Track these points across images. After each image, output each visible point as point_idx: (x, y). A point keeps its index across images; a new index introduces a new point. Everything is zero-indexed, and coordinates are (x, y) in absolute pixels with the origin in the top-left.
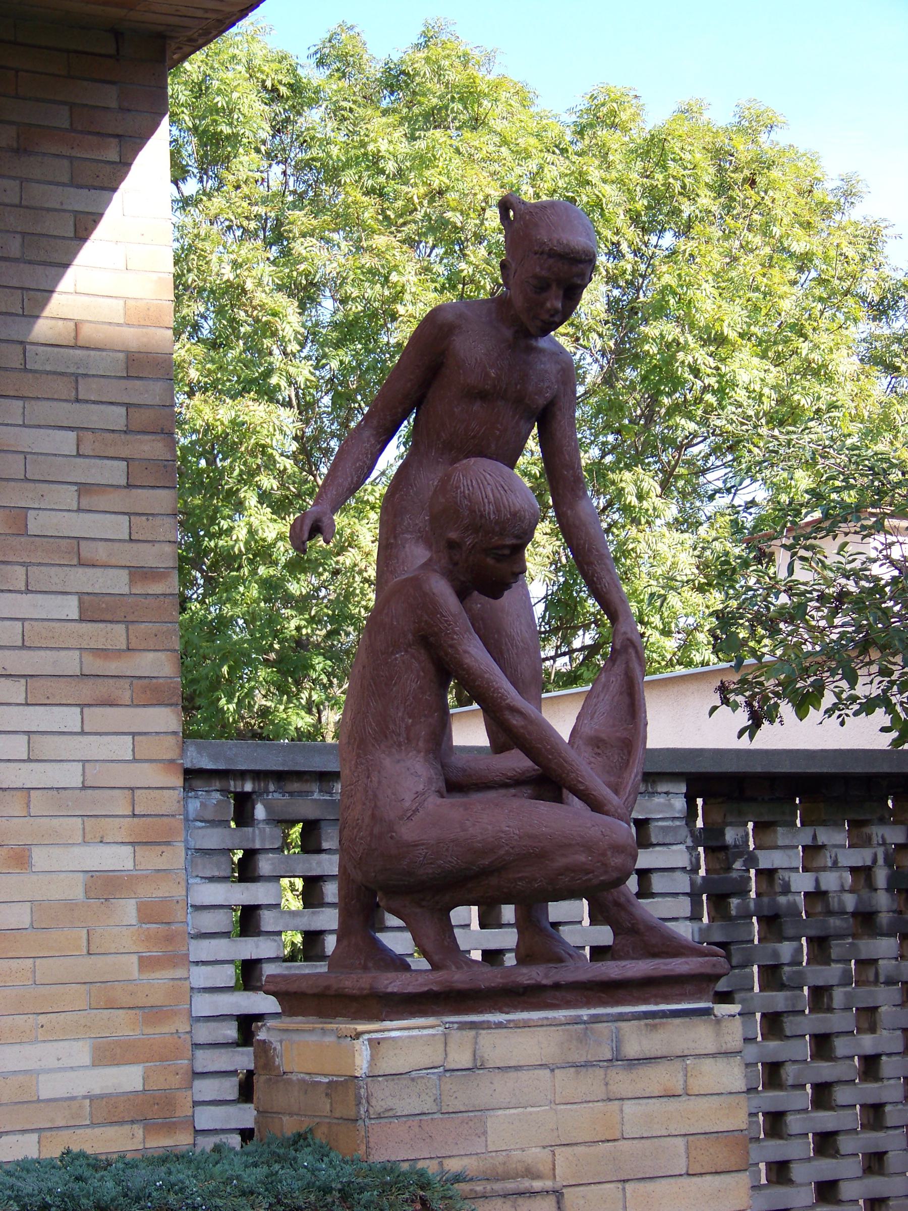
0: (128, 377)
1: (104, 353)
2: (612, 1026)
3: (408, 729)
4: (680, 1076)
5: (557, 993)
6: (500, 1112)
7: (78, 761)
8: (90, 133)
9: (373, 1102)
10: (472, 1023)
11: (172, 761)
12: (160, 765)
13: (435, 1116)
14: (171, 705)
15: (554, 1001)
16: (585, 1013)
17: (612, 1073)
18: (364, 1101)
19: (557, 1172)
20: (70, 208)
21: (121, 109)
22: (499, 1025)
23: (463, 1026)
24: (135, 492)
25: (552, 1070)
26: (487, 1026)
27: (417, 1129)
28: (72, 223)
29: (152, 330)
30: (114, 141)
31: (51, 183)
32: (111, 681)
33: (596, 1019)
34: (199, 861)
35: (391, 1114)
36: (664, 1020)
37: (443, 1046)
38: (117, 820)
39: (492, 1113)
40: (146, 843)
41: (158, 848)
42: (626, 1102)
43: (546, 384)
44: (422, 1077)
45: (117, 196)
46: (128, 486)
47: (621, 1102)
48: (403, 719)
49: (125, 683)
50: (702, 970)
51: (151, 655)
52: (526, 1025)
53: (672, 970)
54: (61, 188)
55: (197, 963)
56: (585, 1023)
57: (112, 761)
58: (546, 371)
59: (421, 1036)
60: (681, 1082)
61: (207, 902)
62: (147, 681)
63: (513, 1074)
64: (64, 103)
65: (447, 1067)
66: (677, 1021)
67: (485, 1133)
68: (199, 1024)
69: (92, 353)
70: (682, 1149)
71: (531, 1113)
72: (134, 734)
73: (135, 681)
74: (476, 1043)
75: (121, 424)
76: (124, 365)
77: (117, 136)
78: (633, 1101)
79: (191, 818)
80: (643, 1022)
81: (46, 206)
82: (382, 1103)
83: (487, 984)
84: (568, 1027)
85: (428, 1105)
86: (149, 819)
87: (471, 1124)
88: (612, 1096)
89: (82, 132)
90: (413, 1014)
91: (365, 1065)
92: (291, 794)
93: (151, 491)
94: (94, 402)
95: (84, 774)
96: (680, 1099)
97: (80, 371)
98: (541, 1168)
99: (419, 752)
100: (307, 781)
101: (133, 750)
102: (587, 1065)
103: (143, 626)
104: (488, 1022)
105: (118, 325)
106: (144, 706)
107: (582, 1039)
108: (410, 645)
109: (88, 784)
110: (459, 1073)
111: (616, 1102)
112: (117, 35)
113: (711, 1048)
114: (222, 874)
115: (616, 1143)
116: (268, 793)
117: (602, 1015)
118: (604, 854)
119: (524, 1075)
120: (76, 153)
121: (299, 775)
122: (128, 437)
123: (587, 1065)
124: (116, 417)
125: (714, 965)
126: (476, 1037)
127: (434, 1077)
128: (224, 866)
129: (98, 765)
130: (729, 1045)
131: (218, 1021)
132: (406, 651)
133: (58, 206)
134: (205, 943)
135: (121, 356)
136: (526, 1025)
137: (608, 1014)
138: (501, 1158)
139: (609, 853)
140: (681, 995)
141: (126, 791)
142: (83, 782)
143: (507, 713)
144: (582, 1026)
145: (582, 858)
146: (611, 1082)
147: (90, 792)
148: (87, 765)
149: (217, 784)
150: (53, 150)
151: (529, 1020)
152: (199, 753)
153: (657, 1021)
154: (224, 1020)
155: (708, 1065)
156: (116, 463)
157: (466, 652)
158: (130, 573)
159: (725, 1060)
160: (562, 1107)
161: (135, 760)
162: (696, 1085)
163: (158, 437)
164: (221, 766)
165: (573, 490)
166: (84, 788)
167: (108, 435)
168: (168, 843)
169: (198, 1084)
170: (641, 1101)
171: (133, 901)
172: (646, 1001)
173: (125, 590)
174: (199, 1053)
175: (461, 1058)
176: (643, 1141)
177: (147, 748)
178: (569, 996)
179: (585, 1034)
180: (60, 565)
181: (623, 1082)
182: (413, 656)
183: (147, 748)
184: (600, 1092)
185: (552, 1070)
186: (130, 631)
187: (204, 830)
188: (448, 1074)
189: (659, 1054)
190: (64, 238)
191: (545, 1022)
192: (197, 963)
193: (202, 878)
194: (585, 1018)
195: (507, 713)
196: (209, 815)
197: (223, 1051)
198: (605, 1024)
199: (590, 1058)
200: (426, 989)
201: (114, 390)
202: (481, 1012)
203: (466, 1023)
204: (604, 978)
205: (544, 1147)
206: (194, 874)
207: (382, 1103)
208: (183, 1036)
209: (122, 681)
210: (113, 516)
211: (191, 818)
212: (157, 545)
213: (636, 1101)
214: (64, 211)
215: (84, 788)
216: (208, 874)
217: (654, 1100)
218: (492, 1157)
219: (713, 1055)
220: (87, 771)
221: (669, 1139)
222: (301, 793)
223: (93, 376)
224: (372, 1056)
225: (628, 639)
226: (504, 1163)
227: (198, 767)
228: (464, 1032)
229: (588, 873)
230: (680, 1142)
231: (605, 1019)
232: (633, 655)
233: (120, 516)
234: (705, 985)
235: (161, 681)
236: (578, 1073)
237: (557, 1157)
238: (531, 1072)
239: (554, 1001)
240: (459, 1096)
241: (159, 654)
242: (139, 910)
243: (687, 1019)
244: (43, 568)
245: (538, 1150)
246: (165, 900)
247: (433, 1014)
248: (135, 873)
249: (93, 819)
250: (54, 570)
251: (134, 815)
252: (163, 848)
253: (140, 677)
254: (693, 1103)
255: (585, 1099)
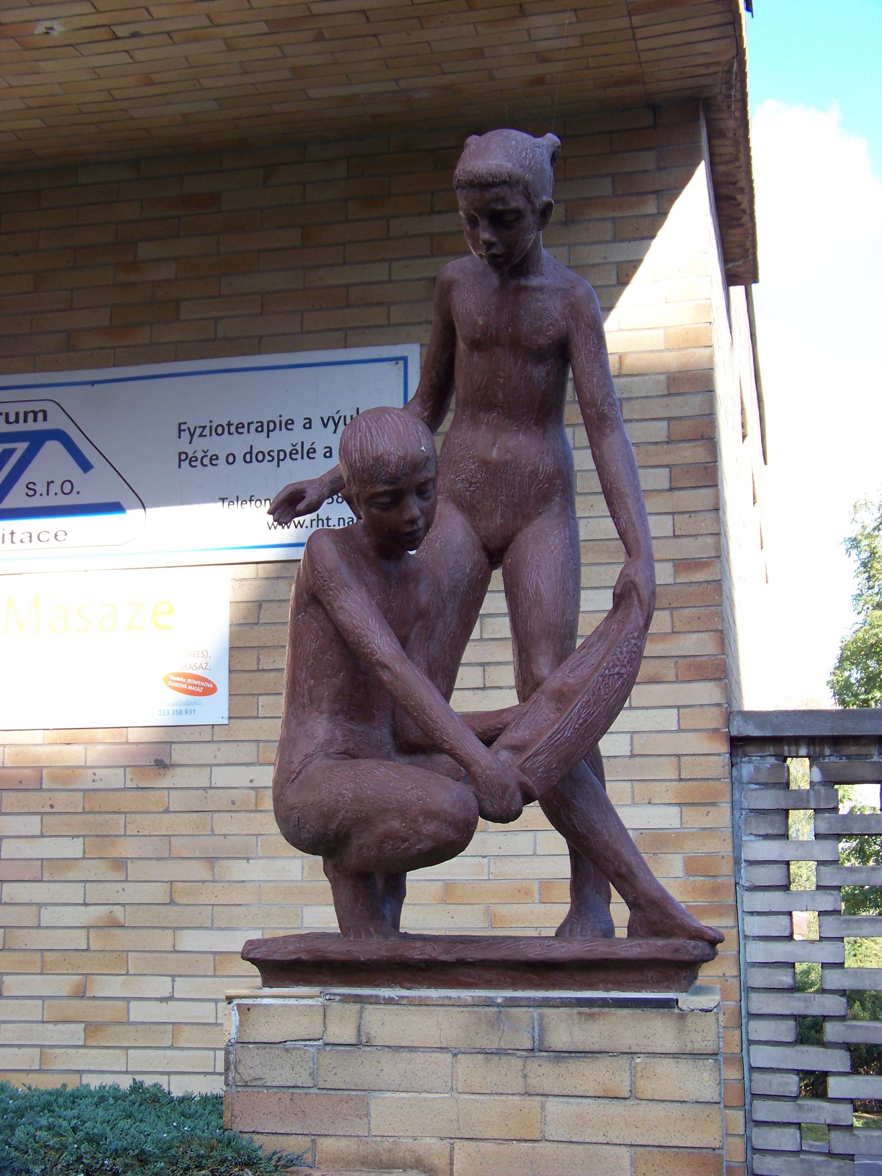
0: (669, 395)
1: (647, 378)
2: (536, 1012)
3: (310, 690)
4: (626, 1076)
5: (472, 971)
6: (388, 1094)
7: (627, 732)
8: (631, 195)
9: (241, 1069)
10: (357, 996)
11: (716, 730)
12: (705, 734)
13: (312, 1091)
14: (715, 680)
15: (473, 981)
16: (500, 995)
17: (533, 1065)
18: (232, 1067)
19: (455, 1168)
20: (612, 260)
21: (659, 169)
22: (390, 1001)
23: (345, 999)
24: (677, 493)
25: (455, 1055)
26: (375, 1000)
27: (288, 1102)
28: (614, 272)
29: (691, 351)
30: (652, 197)
31: (595, 243)
32: (657, 661)
33: (513, 1003)
34: (753, 820)
35: (259, 1083)
36: (606, 1010)
37: (321, 1018)
38: (665, 784)
39: (377, 1094)
40: (693, 804)
41: (703, 808)
42: (551, 1099)
43: (546, 323)
44: (298, 1049)
45: (655, 243)
46: (671, 489)
47: (544, 1099)
48: (306, 680)
49: (670, 663)
50: (659, 955)
51: (695, 636)
52: (422, 1003)
53: (614, 953)
54: (604, 246)
55: (752, 913)
56: (499, 1005)
57: (659, 732)
58: (546, 309)
59: (296, 1006)
60: (628, 1083)
61: (760, 858)
62: (691, 659)
63: (405, 1055)
64: (607, 175)
65: (328, 1040)
66: (624, 1012)
67: (367, 1115)
68: (754, 970)
69: (636, 379)
70: (626, 1162)
71: (425, 1099)
72: (679, 707)
73: (680, 660)
74: (361, 1018)
75: (663, 436)
76: (665, 385)
77: (656, 192)
78: (562, 1099)
79: (745, 781)
80: (575, 1010)
81: (592, 262)
82: (251, 1071)
83: (368, 956)
84: (476, 1009)
85: (303, 1079)
86: (695, 783)
87: (351, 1103)
88: (531, 1090)
89: (623, 195)
90: (297, 982)
91: (234, 1031)
92: (848, 757)
93: (693, 492)
94: (638, 421)
95: (632, 744)
96: (627, 1102)
97: (624, 396)
98: (436, 1162)
99: (321, 713)
100: (865, 745)
101: (678, 721)
102: (499, 1052)
103: (687, 611)
104: (377, 996)
105: (659, 351)
106: (689, 681)
107: (495, 1023)
108: (307, 605)
109: (636, 752)
110: (342, 1048)
111: (539, 1098)
112: (654, 108)
113: (671, 1046)
114: (776, 832)
115: (536, 1144)
116: (824, 757)
117: (521, 998)
118: (415, 821)
119: (419, 1057)
120: (618, 214)
121: (856, 740)
122: (670, 446)
123: (499, 1052)
124: (660, 430)
125: (677, 950)
126: (361, 1012)
127: (312, 1050)
128: (777, 825)
129: (645, 735)
130: (696, 1045)
131: (774, 968)
132: (306, 611)
133: (601, 261)
134: (759, 895)
135: (663, 378)
136: (422, 1003)
137: (529, 998)
138: (387, 1144)
139: (421, 819)
140: (641, 982)
141: (673, 758)
142: (631, 751)
143: (379, 669)
144: (495, 1009)
145: (396, 824)
146: (530, 1074)
147: (638, 759)
148: (635, 736)
149: (771, 750)
150: (597, 216)
151: (427, 998)
152: (745, 721)
153: (596, 1010)
154: (779, 967)
155: (665, 1066)
156: (659, 470)
157: (340, 608)
158: (675, 566)
159: (691, 1062)
160: (466, 1096)
161: (680, 730)
162: (647, 1088)
163: (699, 443)
164: (768, 733)
165: (598, 428)
166: (633, 756)
167: (651, 448)
168: (713, 804)
169: (754, 1025)
170: (571, 1100)
171: (680, 856)
172: (592, 987)
173: (670, 580)
174: (754, 996)
175: (342, 1030)
176: (572, 1146)
177: (691, 719)
178: (489, 975)
179: (498, 1018)
180: (609, 564)
181: (545, 1075)
182: (312, 617)
183: (691, 719)
184: (517, 1085)
185: (455, 1055)
186: (675, 616)
187: (758, 792)
188: (328, 1048)
189: (596, 1048)
190: (608, 286)
191: (446, 1002)
192: (752, 913)
193: (756, 835)
194: (499, 1001)
195: (379, 669)
196: (762, 778)
197: (774, 995)
198: (525, 1009)
199: (503, 1045)
200: (294, 957)
201: (656, 408)
202: (378, 986)
203: (350, 995)
204: (520, 957)
205: (441, 1139)
206: (748, 832)
207: (251, 1071)
208: (730, 980)
209: (668, 661)
210: (658, 517)
211: (745, 781)
212: (700, 538)
213: (566, 1099)
214: (608, 263)
215: (633, 756)
216: (762, 832)
217: (589, 1100)
218: (375, 1142)
219: (674, 1055)
220: (634, 741)
221: (608, 1147)
222: (859, 757)
223: (637, 398)
224: (241, 1021)
225: (631, 582)
226: (390, 1151)
227: (745, 734)
228: (346, 1005)
229: (404, 842)
230: (624, 1154)
231: (524, 1003)
232: (636, 598)
233: (664, 517)
234: (673, 973)
235: (704, 658)
236: (487, 1059)
237: (456, 1151)
238: (428, 1055)
239: (473, 981)
240: (339, 1072)
241: (703, 634)
242: (685, 863)
243: (639, 1011)
244: (593, 568)
245: (434, 1140)
246: (710, 855)
247: (320, 983)
248: (682, 831)
249: (642, 784)
250: (603, 568)
251: (681, 780)
252: (708, 808)
253: (685, 657)
254: (641, 1109)
255: (495, 1090)
